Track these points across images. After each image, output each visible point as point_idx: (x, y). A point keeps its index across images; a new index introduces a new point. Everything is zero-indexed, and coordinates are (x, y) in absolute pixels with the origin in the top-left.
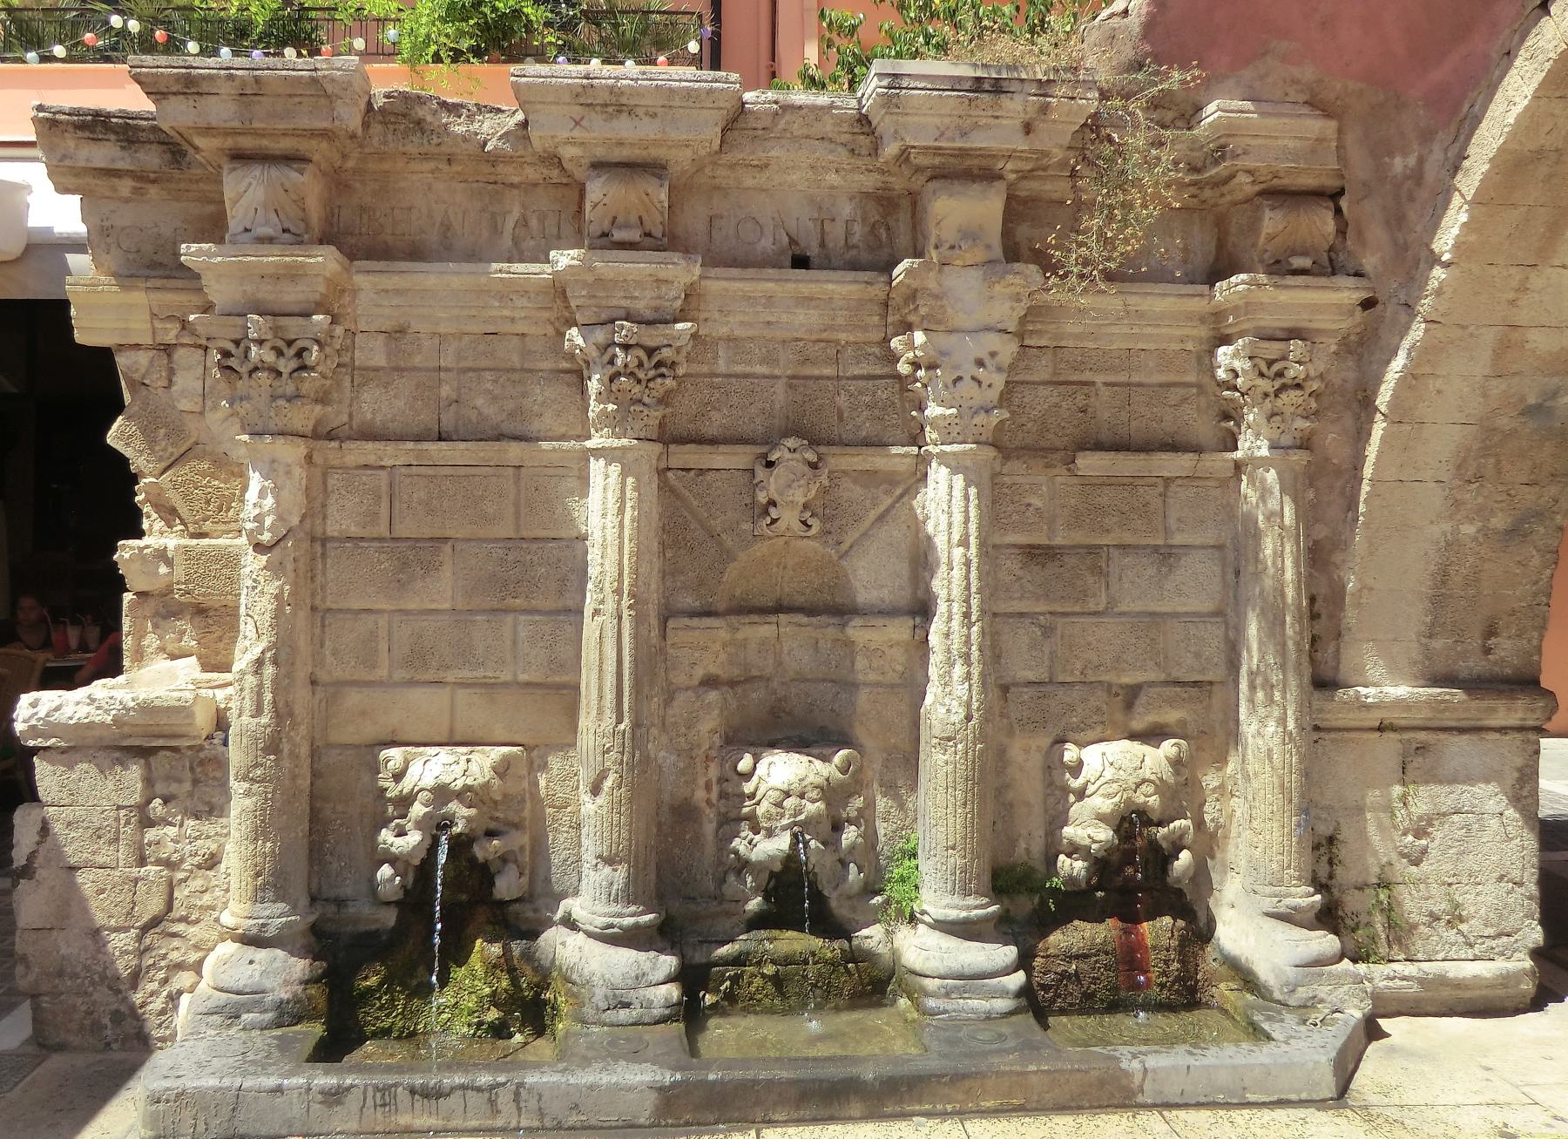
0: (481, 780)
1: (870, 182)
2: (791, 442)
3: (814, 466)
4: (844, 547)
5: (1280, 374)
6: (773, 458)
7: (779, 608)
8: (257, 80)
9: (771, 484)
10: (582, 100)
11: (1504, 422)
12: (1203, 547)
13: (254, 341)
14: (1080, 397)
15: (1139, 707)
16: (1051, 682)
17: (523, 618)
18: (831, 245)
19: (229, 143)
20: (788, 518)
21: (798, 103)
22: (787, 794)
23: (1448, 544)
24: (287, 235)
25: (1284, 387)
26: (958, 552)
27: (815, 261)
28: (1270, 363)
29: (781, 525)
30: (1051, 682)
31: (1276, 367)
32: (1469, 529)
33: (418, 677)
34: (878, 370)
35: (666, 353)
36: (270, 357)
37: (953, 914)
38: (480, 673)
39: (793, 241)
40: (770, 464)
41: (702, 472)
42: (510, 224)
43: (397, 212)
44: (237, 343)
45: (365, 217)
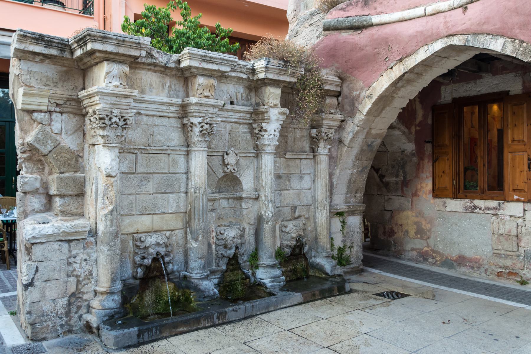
0: (166, 241)
2: (232, 149)
6: (228, 152)
8: (124, 41)
10: (203, 58)
11: (364, 148)
13: (115, 116)
14: (285, 139)
15: (297, 213)
17: (170, 195)
18: (238, 99)
19: (107, 56)
21: (240, 64)
22: (234, 238)
24: (122, 85)
26: (269, 177)
27: (235, 103)
31: (327, 134)
32: (355, 171)
33: (144, 213)
35: (214, 125)
36: (118, 121)
37: (271, 263)
40: (227, 154)
42: (167, 86)
43: (138, 79)
44: (107, 116)
45: (129, 80)
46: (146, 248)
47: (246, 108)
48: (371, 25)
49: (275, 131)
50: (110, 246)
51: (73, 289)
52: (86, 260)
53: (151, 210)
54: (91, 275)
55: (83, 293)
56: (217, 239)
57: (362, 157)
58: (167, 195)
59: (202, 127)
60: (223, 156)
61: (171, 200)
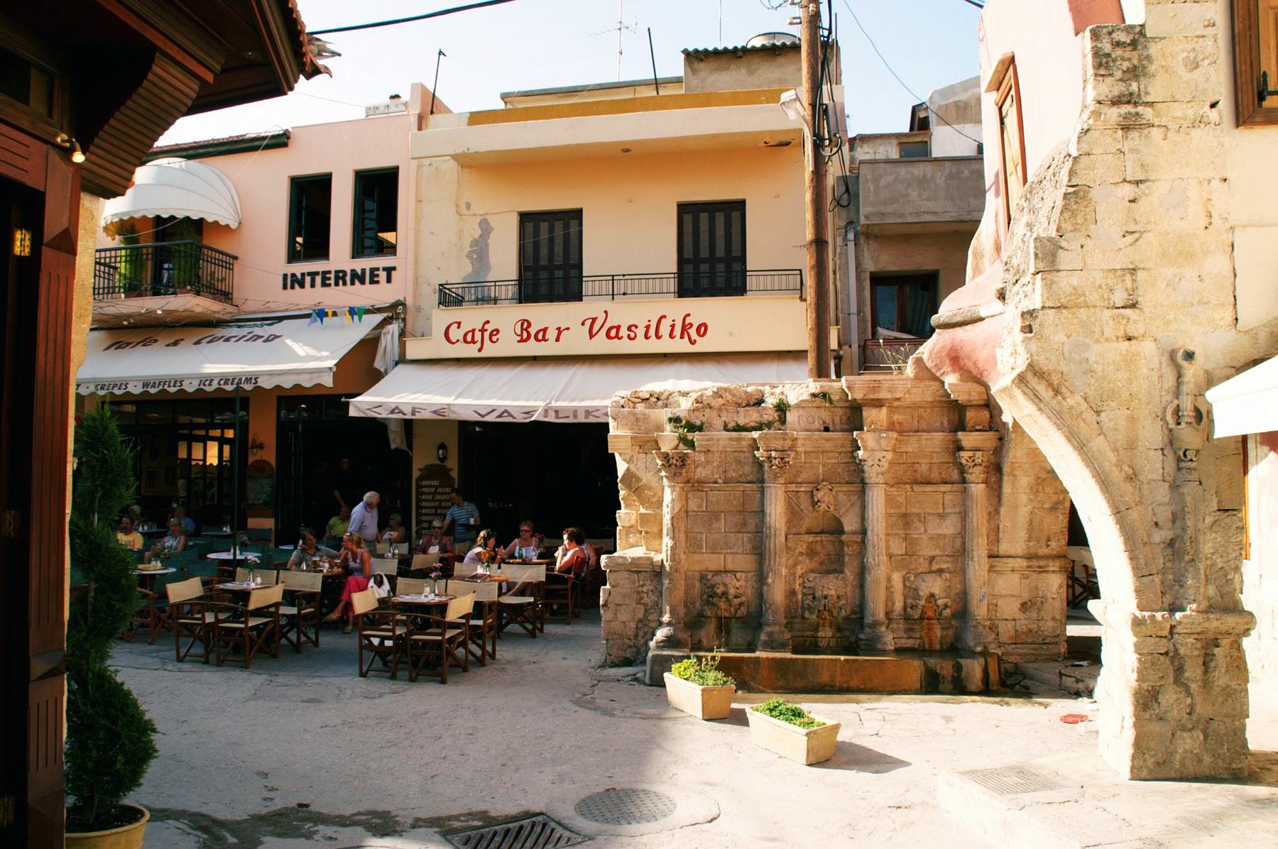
1: (846, 404)
2: (824, 483)
3: (831, 490)
4: (842, 512)
5: (973, 461)
7: (822, 532)
9: (819, 495)
12: (955, 513)
15: (934, 564)
16: (906, 554)
17: (745, 535)
20: (823, 506)
23: (1031, 513)
25: (975, 465)
27: (831, 428)
28: (970, 458)
29: (821, 508)
30: (906, 554)
34: (850, 460)
36: (675, 462)
38: (733, 551)
39: (824, 422)
40: (818, 490)
41: (798, 492)
46: (713, 586)
47: (837, 433)
48: (982, 319)
49: (880, 460)
50: (670, 580)
51: (640, 615)
52: (652, 591)
53: (721, 549)
54: (657, 605)
55: (650, 621)
56: (805, 587)
57: (1043, 489)
58: (741, 535)
59: (771, 462)
60: (812, 492)
61: (745, 539)
